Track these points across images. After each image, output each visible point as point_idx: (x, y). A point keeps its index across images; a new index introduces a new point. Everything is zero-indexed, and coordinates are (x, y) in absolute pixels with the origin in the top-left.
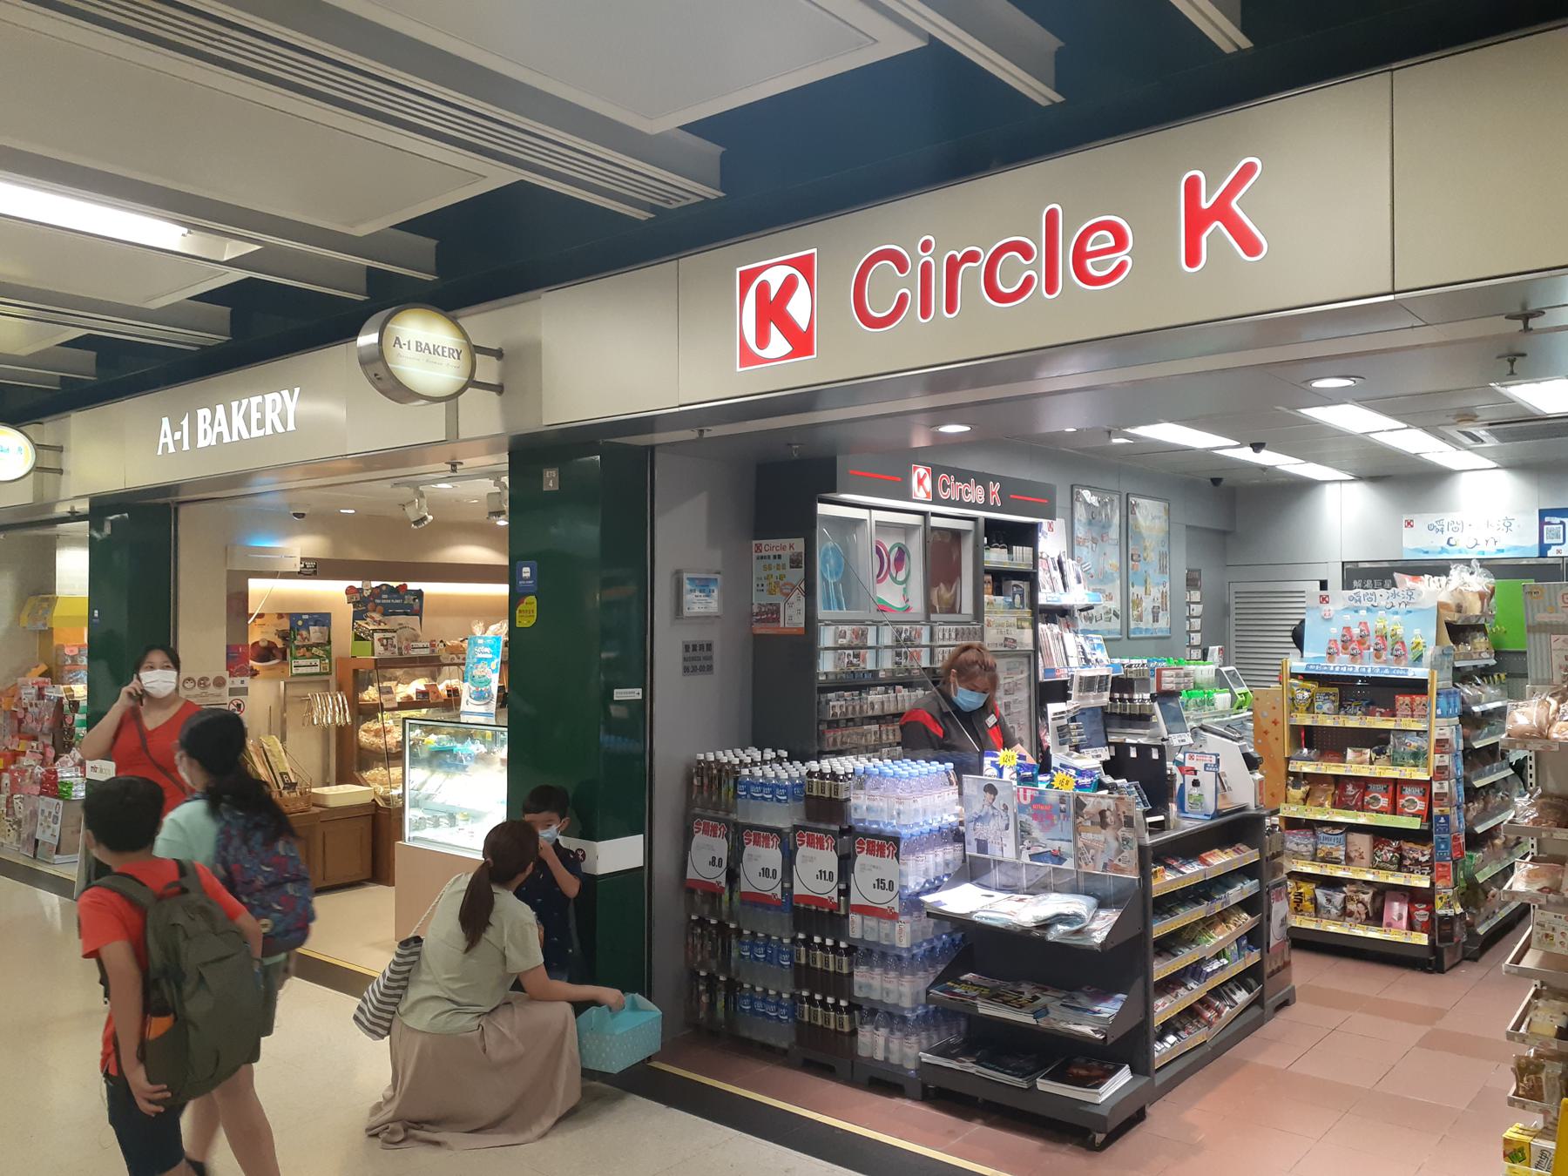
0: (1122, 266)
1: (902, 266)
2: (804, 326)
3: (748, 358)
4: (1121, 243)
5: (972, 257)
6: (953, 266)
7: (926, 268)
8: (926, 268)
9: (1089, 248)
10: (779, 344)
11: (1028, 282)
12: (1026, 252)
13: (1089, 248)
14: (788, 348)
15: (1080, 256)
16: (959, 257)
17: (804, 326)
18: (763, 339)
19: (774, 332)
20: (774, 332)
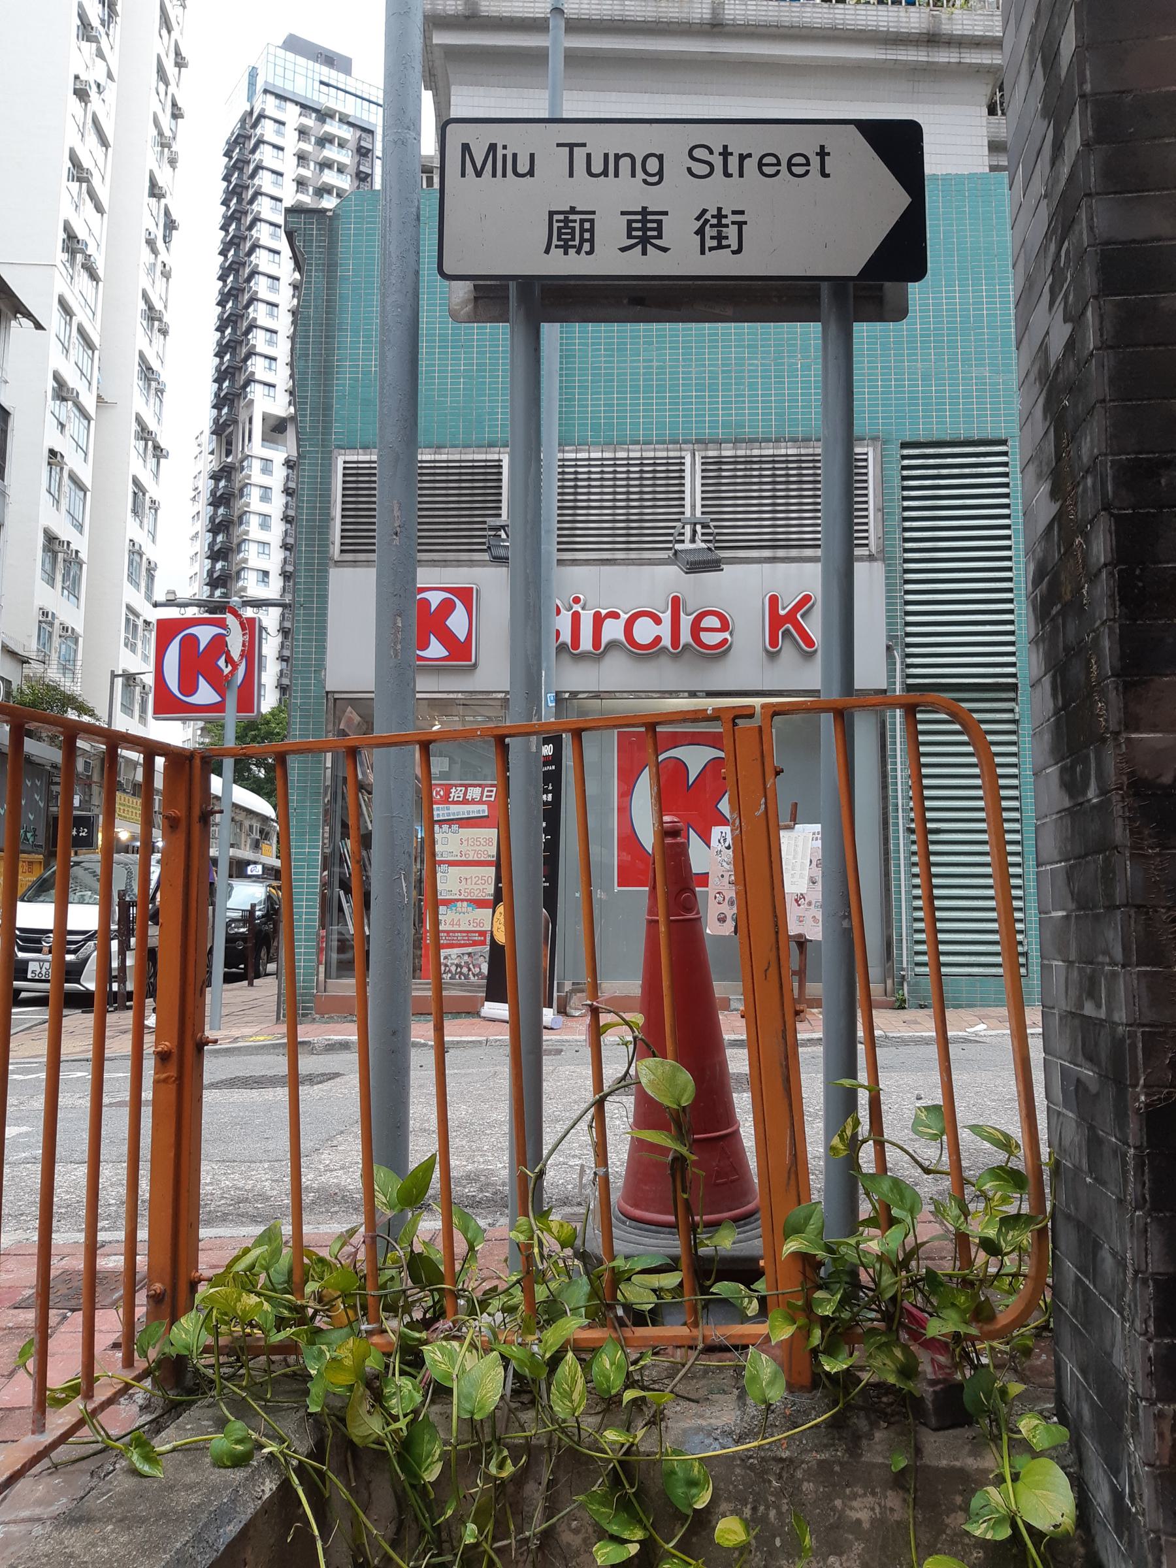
0: (725, 640)
2: (462, 640)
4: (725, 626)
5: (615, 615)
6: (598, 620)
7: (576, 617)
8: (576, 617)
10: (436, 649)
11: (658, 639)
12: (658, 621)
14: (443, 652)
15: (696, 629)
16: (604, 612)
17: (462, 640)
19: (433, 638)
20: (433, 638)
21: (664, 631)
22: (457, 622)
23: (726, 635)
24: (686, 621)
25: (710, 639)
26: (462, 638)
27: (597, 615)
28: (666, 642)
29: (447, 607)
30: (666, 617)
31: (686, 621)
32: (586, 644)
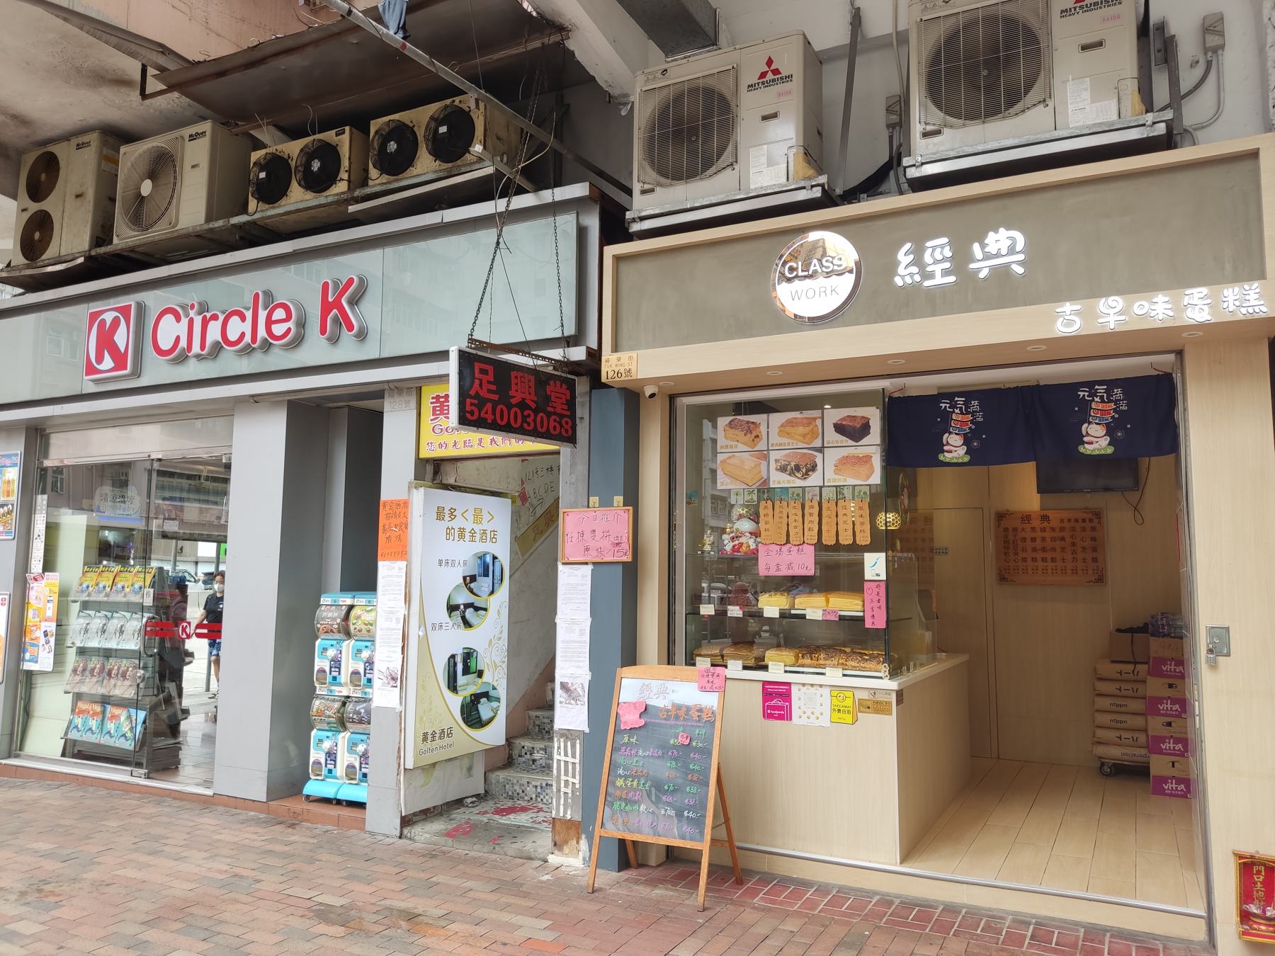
0: (289, 330)
1: (178, 319)
2: (123, 350)
3: (91, 370)
5: (215, 317)
7: (191, 322)
8: (191, 322)
9: (274, 318)
10: (108, 363)
11: (243, 335)
12: (243, 319)
13: (274, 318)
15: (269, 322)
16: (208, 315)
18: (100, 359)
21: (247, 327)
22: (121, 338)
23: (291, 324)
24: (262, 315)
25: (278, 329)
26: (123, 350)
27: (205, 317)
28: (248, 338)
29: (116, 322)
30: (249, 314)
31: (262, 315)
32: (196, 348)
